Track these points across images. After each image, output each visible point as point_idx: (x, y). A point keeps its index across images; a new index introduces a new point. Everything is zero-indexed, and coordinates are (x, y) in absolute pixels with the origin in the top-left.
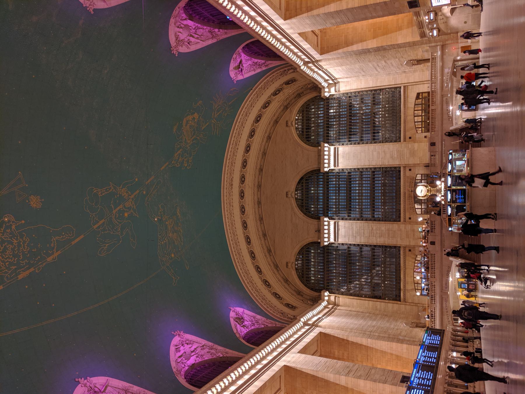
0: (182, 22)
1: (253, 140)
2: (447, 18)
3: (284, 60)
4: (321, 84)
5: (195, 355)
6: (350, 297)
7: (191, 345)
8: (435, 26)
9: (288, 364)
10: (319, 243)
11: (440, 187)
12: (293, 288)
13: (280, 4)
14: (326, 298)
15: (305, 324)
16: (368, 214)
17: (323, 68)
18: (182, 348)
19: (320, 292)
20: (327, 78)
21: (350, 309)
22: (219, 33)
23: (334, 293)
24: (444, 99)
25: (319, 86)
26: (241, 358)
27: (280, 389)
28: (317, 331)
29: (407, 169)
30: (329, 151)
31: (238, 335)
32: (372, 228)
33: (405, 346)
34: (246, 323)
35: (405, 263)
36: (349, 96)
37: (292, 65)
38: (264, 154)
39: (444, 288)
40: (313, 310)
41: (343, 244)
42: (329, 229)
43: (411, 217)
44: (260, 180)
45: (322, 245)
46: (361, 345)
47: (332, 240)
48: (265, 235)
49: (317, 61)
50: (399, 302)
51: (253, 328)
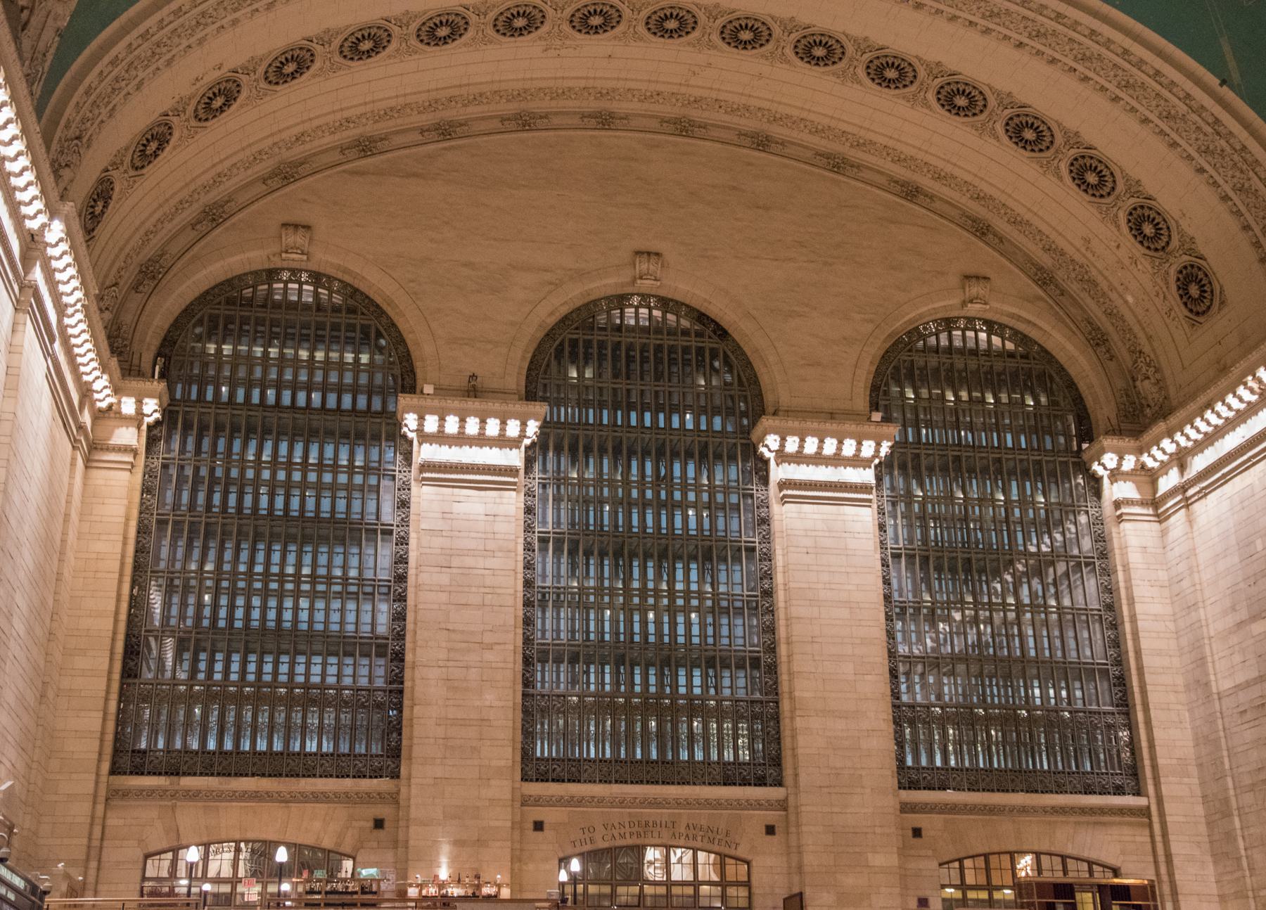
6: (133, 524)
12: (174, 249)
14: (128, 406)
16: (556, 626)
21: (74, 516)
25: (1161, 426)
29: (772, 816)
32: (490, 647)
35: (317, 797)
36: (1102, 559)
41: (404, 504)
42: (481, 440)
43: (548, 833)
44: (715, 133)
47: (426, 453)
48: (445, 131)
50: (106, 766)
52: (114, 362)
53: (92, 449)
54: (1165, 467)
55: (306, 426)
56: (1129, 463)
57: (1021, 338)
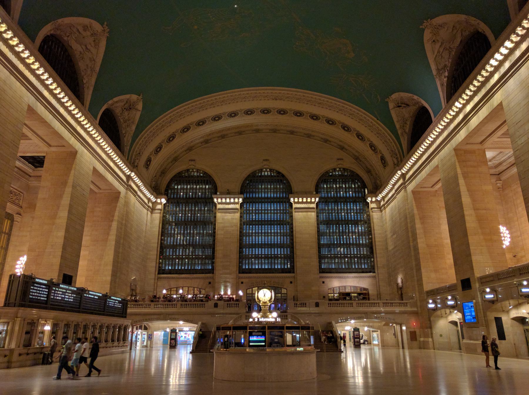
0: (459, 31)
1: (324, 123)
2: (446, 317)
3: (408, 153)
5: (82, 50)
6: (161, 224)
7: (93, 45)
8: (439, 306)
9: (78, 156)
10: (216, 194)
11: (270, 316)
13: (472, 144)
14: (159, 201)
15: (129, 177)
17: (397, 194)
19: (165, 194)
20: (386, 199)
21: (148, 224)
22: (443, 77)
23: (164, 208)
24: (363, 315)
25: (378, 192)
26: (83, 104)
27: (50, 146)
28: (122, 189)
29: (292, 280)
30: (311, 202)
31: (110, 102)
33: (109, 278)
34: (126, 113)
35: (197, 278)
37: (401, 161)
38: (309, 136)
39: (170, 316)
40: (145, 186)
41: (215, 217)
42: (230, 203)
43: (244, 284)
45: (213, 196)
46: (108, 234)
47: (219, 206)
48: (223, 137)
49: (405, 188)
50: (157, 273)
51: (122, 120)
52: (154, 193)
54: (381, 200)
55: (195, 201)
56: (374, 199)
57: (352, 172)
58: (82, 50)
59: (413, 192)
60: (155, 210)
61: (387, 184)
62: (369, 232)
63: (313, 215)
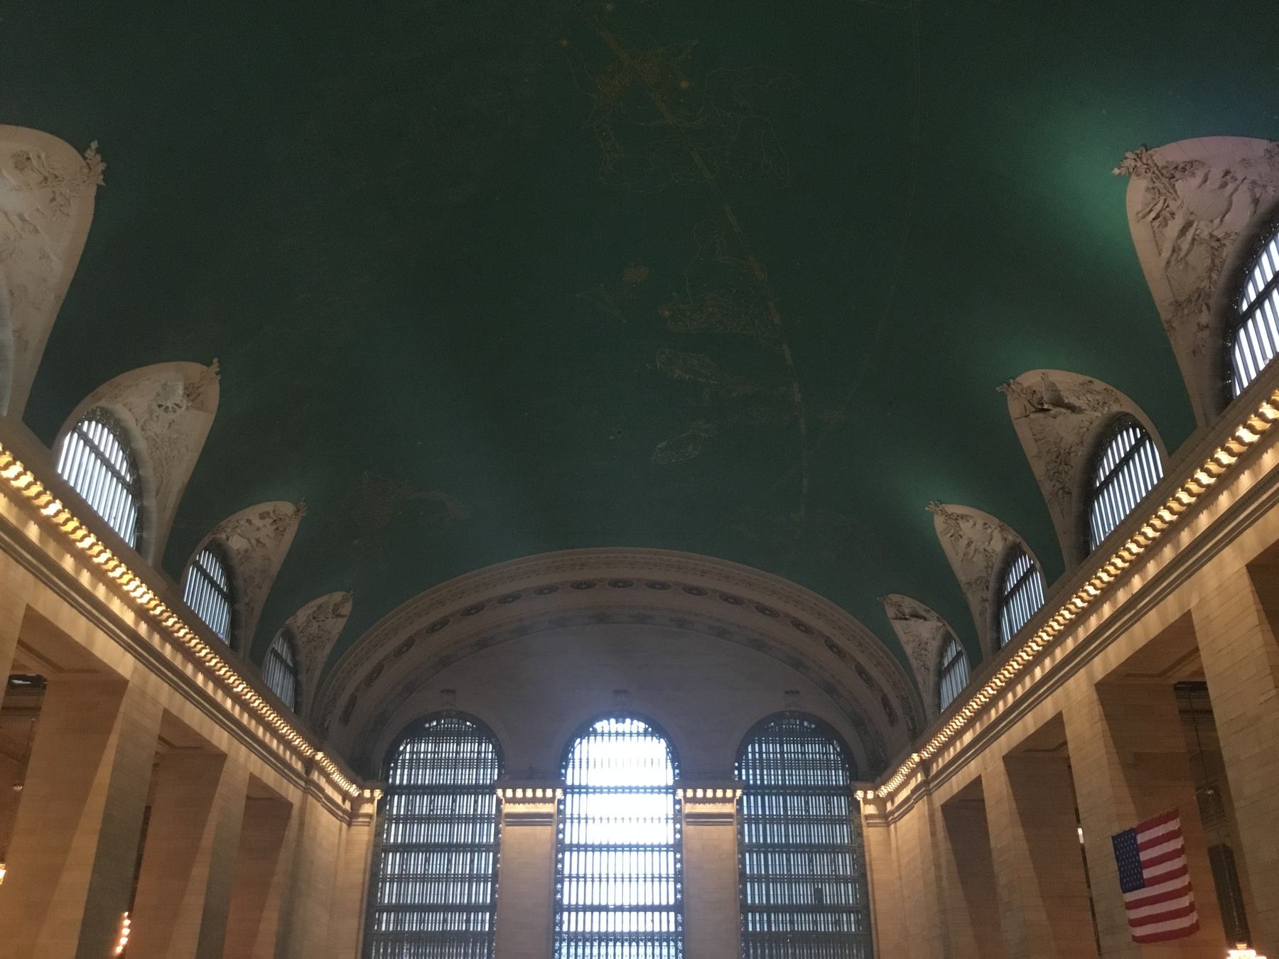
4: (884, 783)
5: (249, 546)
9: (228, 765)
14: (367, 793)
15: (310, 764)
17: (916, 801)
18: (269, 521)
25: (878, 779)
30: (724, 800)
34: (315, 624)
42: (534, 800)
49: (929, 793)
52: (359, 779)
53: (351, 817)
56: (870, 795)
58: (249, 546)
59: (944, 807)
60: (359, 816)
61: (894, 773)
62: (861, 877)
63: (729, 832)
